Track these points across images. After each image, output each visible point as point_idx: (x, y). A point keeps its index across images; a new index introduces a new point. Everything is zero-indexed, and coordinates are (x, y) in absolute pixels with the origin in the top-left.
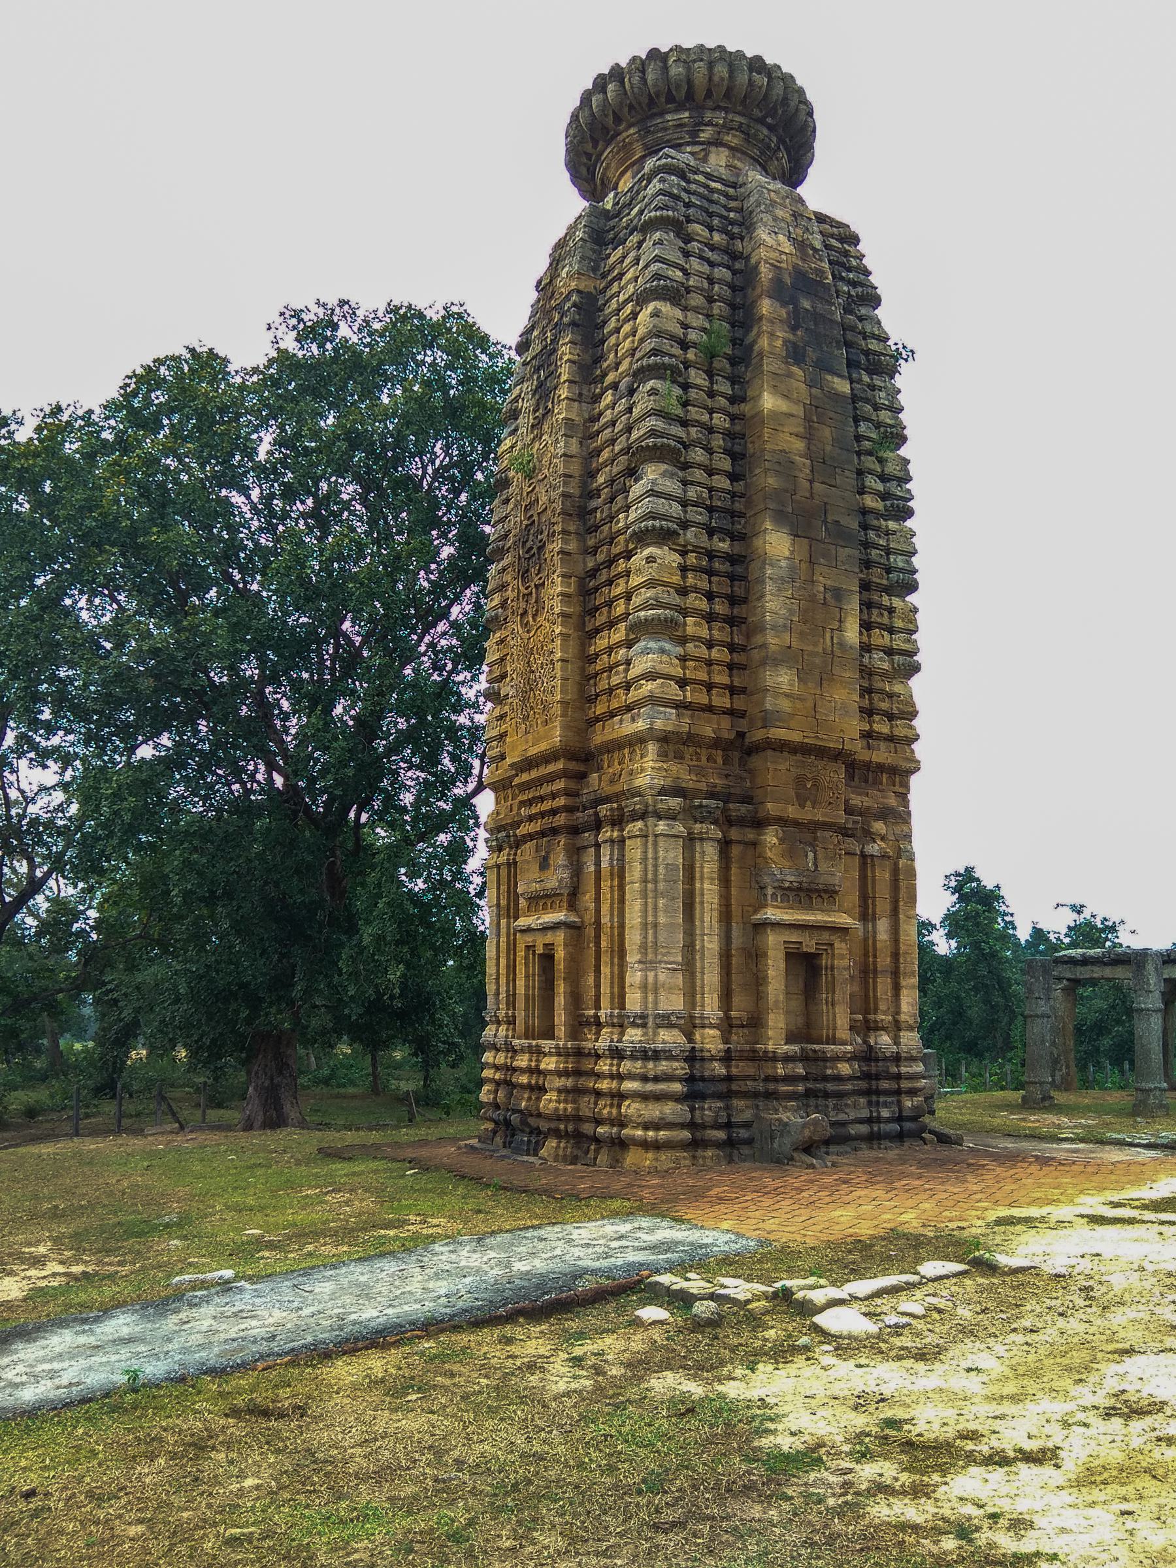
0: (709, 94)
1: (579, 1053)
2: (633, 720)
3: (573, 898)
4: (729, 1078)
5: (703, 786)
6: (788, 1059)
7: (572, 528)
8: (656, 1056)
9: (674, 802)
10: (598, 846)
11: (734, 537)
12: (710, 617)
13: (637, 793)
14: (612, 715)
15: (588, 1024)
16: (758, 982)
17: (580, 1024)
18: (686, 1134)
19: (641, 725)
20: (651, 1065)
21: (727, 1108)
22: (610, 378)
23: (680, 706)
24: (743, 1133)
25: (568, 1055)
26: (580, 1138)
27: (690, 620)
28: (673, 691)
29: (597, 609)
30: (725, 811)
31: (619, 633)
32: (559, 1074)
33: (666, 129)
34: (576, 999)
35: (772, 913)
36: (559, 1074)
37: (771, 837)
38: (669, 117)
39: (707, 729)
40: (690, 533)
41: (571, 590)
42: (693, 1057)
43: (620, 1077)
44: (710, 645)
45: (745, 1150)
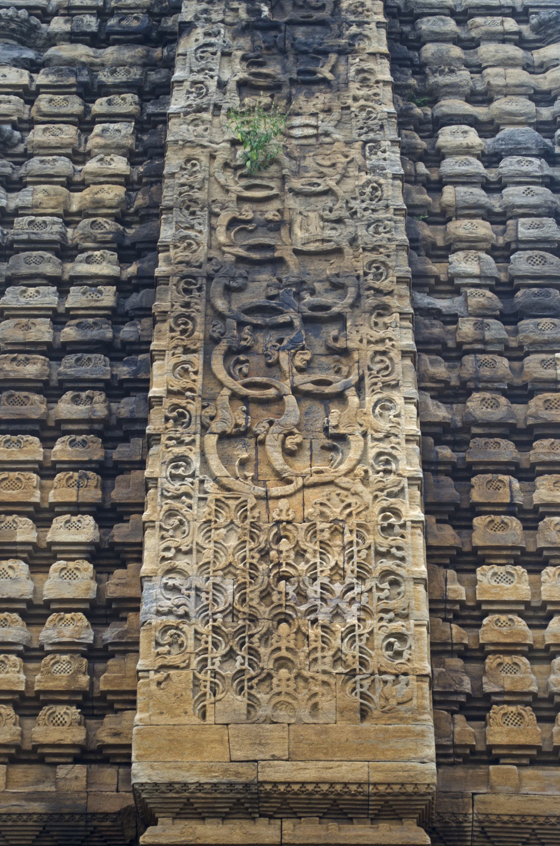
29: (476, 510)
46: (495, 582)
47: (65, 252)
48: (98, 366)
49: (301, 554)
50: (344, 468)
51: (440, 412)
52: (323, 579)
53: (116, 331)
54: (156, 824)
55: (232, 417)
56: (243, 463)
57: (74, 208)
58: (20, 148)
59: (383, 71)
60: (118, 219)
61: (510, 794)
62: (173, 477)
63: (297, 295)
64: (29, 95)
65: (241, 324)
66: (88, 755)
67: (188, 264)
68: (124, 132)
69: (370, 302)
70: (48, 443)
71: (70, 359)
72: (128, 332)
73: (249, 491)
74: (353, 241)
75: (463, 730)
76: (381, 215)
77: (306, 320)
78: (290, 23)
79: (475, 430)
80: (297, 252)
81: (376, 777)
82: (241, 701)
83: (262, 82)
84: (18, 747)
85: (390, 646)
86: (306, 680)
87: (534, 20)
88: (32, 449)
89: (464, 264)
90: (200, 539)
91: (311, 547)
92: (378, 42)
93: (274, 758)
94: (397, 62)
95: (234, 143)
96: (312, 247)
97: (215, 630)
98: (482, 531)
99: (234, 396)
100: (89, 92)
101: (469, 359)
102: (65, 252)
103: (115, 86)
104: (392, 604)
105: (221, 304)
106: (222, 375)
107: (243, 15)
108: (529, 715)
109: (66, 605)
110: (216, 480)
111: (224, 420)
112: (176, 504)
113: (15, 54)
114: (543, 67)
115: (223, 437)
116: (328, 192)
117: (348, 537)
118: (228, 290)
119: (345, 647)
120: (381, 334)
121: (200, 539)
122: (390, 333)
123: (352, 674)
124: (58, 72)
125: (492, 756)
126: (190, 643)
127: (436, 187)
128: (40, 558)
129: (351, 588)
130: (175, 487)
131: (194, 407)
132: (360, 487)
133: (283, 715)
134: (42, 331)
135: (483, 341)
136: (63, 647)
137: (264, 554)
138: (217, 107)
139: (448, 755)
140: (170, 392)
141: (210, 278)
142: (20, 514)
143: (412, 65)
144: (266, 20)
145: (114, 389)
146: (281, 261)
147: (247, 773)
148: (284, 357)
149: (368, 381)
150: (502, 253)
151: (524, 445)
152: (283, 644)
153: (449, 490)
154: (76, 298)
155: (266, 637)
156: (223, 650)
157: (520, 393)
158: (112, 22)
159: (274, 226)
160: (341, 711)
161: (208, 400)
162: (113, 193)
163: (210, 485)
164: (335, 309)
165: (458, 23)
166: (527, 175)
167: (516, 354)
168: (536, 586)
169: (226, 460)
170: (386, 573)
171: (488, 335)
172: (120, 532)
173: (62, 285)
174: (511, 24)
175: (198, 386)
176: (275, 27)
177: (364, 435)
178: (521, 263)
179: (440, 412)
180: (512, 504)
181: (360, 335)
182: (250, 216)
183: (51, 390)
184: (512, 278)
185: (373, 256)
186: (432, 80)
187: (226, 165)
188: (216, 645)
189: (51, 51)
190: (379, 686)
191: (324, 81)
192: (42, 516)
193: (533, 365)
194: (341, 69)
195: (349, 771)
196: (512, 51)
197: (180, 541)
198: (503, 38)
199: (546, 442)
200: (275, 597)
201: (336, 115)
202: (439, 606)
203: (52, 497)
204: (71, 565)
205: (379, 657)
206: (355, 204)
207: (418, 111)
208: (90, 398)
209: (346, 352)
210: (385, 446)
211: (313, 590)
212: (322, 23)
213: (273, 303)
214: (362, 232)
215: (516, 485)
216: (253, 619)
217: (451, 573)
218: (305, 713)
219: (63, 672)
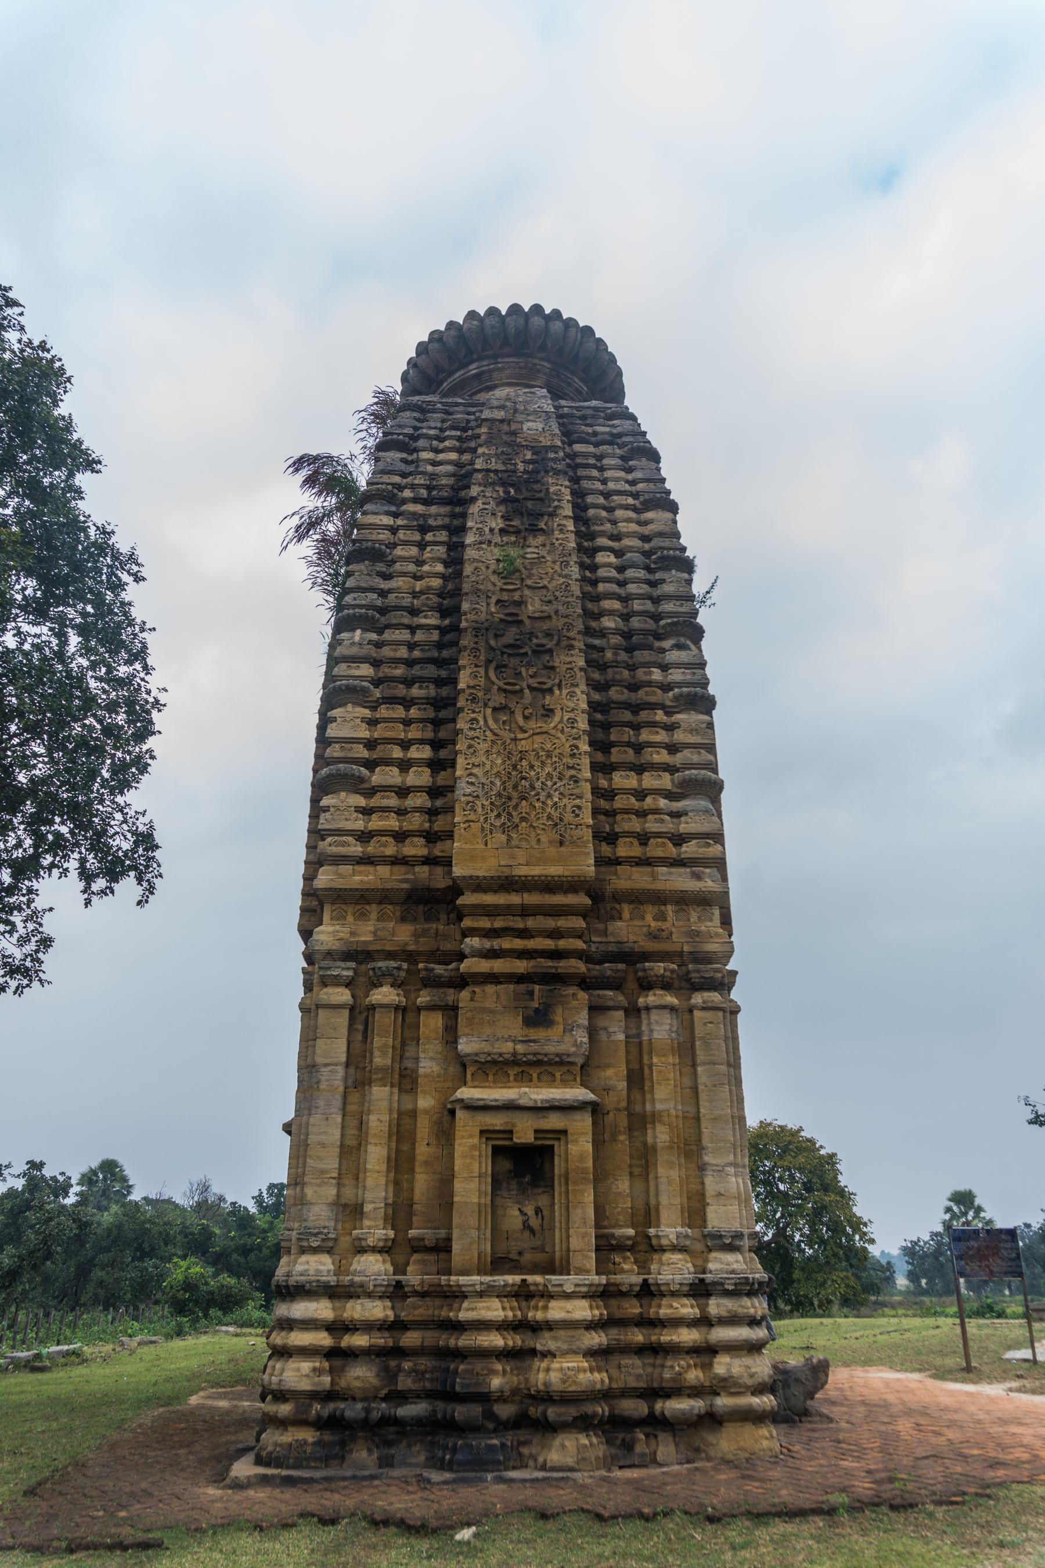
15: (620, 1247)
26: (624, 1425)
29: (612, 744)
31: (666, 781)
32: (591, 1326)
33: (570, 385)
38: (576, 380)
43: (705, 1321)
46: (623, 780)
47: (414, 612)
48: (431, 671)
49: (532, 767)
50: (552, 725)
51: (597, 697)
52: (542, 779)
53: (440, 653)
54: (463, 894)
55: (499, 699)
56: (504, 722)
57: (417, 589)
58: (390, 558)
59: (570, 526)
60: (440, 596)
61: (626, 880)
62: (471, 729)
63: (530, 640)
64: (394, 530)
65: (503, 653)
66: (429, 861)
67: (476, 622)
68: (441, 551)
69: (564, 643)
70: (407, 708)
71: (417, 667)
72: (445, 653)
73: (507, 736)
74: (556, 612)
75: (606, 849)
76: (570, 599)
77: (534, 651)
78: (525, 499)
79: (612, 705)
80: (529, 617)
81: (567, 873)
82: (503, 838)
83: (511, 529)
84: (396, 857)
85: (574, 812)
86: (534, 827)
87: (642, 499)
88: (400, 712)
89: (608, 623)
90: (484, 759)
91: (537, 764)
92: (568, 511)
93: (520, 864)
94: (576, 519)
95: (498, 561)
96: (537, 615)
97: (492, 803)
98: (616, 755)
99: (500, 689)
100: (423, 529)
101: (610, 670)
102: (414, 612)
103: (437, 527)
104: (575, 791)
105: (493, 643)
106: (494, 679)
107: (502, 494)
108: (636, 842)
109: (417, 789)
110: (491, 730)
111: (495, 701)
112: (472, 742)
113: (386, 508)
114: (646, 523)
115: (495, 709)
116: (544, 587)
117: (554, 759)
118: (496, 636)
119: (552, 812)
120: (570, 659)
121: (484, 759)
122: (574, 659)
123: (556, 825)
124: (408, 519)
125: (618, 862)
126: (480, 809)
127: (594, 583)
128: (404, 765)
129: (555, 784)
130: (471, 733)
131: (480, 694)
132: (560, 735)
133: (524, 844)
134: (403, 653)
135: (617, 662)
136: (416, 809)
137: (515, 767)
138: (490, 542)
139: (601, 861)
140: (468, 687)
141: (487, 629)
142: (394, 744)
143: (582, 520)
144: (512, 497)
145: (439, 682)
146: (521, 622)
147: (507, 872)
148: (523, 670)
149: (563, 683)
150: (626, 617)
151: (635, 713)
152: (524, 810)
153: (600, 735)
154: (420, 636)
155: (515, 807)
156: (495, 813)
157: (634, 687)
158: (434, 493)
159: (519, 604)
160: (550, 842)
161: (487, 691)
162: (436, 583)
163: (488, 733)
164: (548, 647)
165: (605, 498)
166: (638, 578)
167: (632, 668)
168: (640, 781)
169: (496, 721)
170: (572, 777)
171: (619, 659)
172: (443, 754)
173: (413, 629)
174: (630, 501)
175: (482, 684)
176: (517, 500)
177: (562, 709)
178: (635, 623)
179: (597, 697)
180: (629, 742)
181: (560, 660)
182: (506, 598)
183: (409, 682)
184: (630, 630)
185: (566, 620)
186: (592, 528)
187: (494, 572)
188: (492, 811)
189: (404, 508)
190: (568, 831)
191: (542, 530)
192: (405, 745)
193: (640, 673)
194: (550, 523)
195: (554, 870)
196: (631, 514)
197: (476, 761)
198: (626, 507)
199: (646, 712)
200: (520, 788)
201: (548, 548)
202: (596, 791)
203: (410, 736)
204: (420, 769)
205: (569, 817)
206: (557, 594)
207: (586, 544)
208: (427, 687)
209: (553, 668)
210: (571, 715)
211: (538, 785)
212: (541, 499)
213: (518, 642)
214: (560, 608)
215: (632, 732)
216: (510, 798)
217: (600, 775)
218: (534, 843)
219: (416, 822)
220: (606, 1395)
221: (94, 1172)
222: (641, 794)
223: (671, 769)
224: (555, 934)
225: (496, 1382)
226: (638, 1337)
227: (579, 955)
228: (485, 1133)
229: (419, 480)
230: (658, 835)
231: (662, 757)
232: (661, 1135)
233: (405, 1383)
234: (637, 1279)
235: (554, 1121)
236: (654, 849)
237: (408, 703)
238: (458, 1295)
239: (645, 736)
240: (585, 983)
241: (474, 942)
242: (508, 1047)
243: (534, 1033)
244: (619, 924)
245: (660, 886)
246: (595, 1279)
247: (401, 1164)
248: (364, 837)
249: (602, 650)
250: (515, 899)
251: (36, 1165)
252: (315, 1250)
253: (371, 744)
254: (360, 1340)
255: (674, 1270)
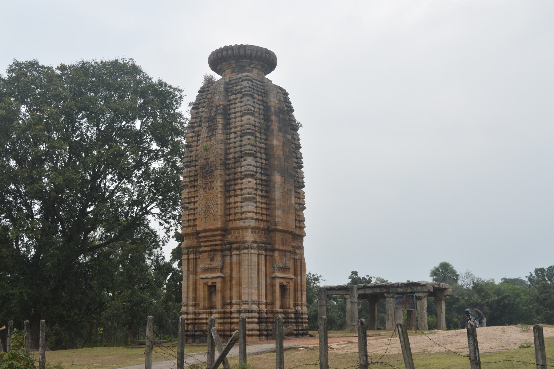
0: (255, 57)
1: (224, 313)
2: (244, 222)
3: (222, 270)
4: (267, 318)
5: (261, 241)
6: (281, 313)
7: (222, 168)
8: (252, 312)
9: (255, 245)
10: (231, 256)
11: (266, 175)
12: (261, 196)
13: (245, 242)
14: (235, 220)
15: (227, 304)
16: (274, 292)
17: (224, 305)
18: (258, 333)
19: (247, 224)
20: (250, 314)
21: (267, 326)
22: (233, 130)
23: (256, 219)
24: (270, 333)
25: (221, 313)
27: (258, 197)
28: (255, 216)
29: (230, 191)
30: (266, 247)
31: (239, 199)
32: (219, 318)
34: (223, 298)
35: (277, 274)
36: (221, 318)
37: (276, 254)
39: (262, 225)
40: (258, 174)
41: (222, 185)
42: (260, 312)
44: (262, 203)
45: (271, 337)
92: (220, 126)
178: (237, 155)
179: (227, 178)
195: (213, 227)
205: (216, 214)
220: (224, 331)
221: (437, 269)
222: (235, 203)
223: (241, 195)
224: (215, 241)
225: (204, 328)
226: (229, 320)
227: (221, 245)
228: (206, 284)
229: (198, 120)
230: (238, 213)
231: (239, 192)
232: (234, 282)
233: (196, 329)
234: (229, 310)
235: (214, 280)
236: (237, 217)
237: (194, 186)
238: (199, 314)
239: (237, 187)
240: (222, 251)
241: (202, 244)
242: (207, 266)
243: (212, 263)
244: (230, 236)
245: (237, 226)
246: (220, 310)
247: (195, 290)
248: (189, 221)
249: (229, 164)
250: (208, 234)
251: (355, 273)
252: (184, 306)
253: (189, 198)
254: (189, 322)
255: (235, 308)
